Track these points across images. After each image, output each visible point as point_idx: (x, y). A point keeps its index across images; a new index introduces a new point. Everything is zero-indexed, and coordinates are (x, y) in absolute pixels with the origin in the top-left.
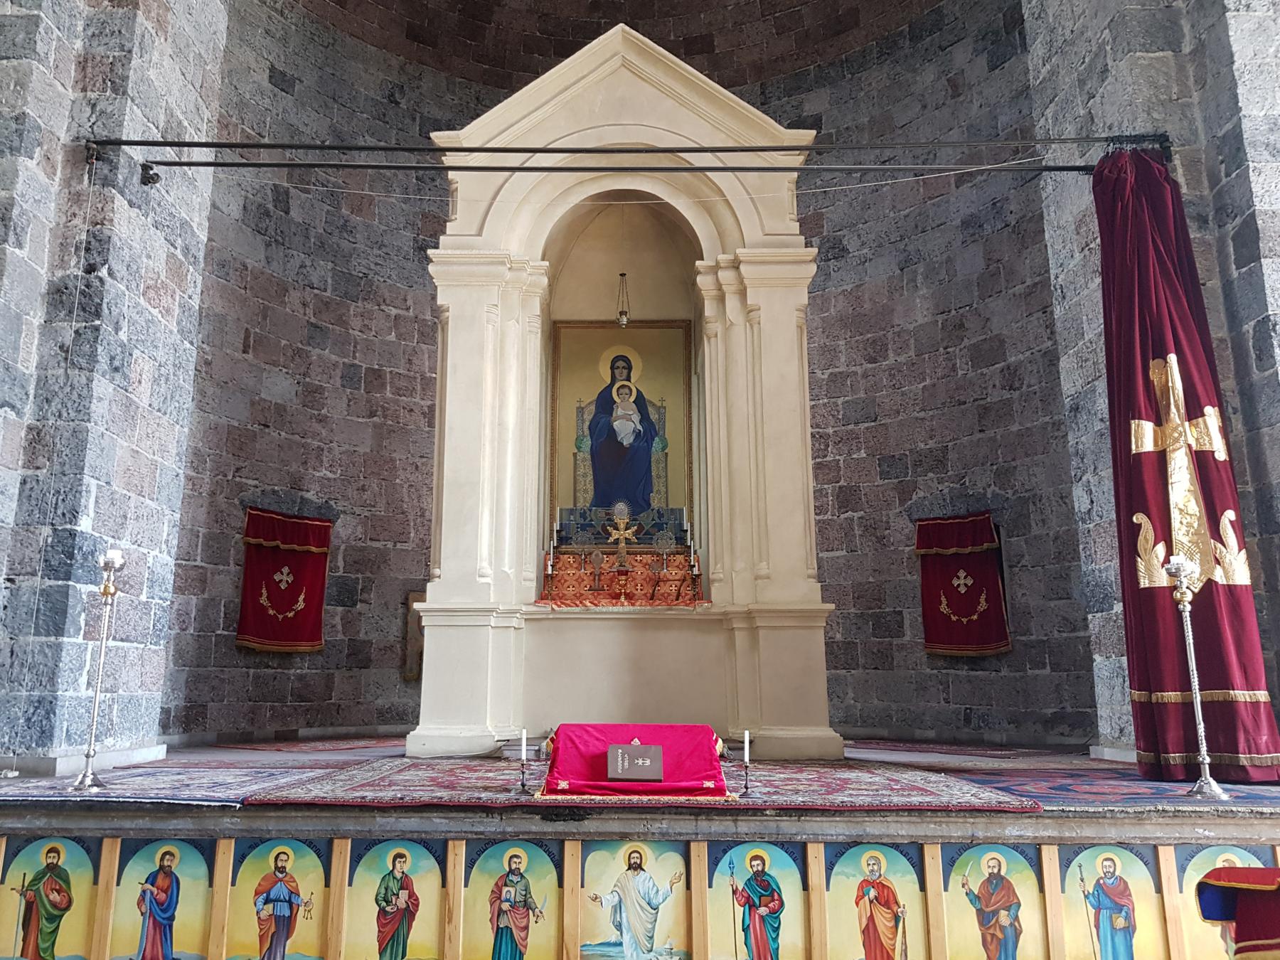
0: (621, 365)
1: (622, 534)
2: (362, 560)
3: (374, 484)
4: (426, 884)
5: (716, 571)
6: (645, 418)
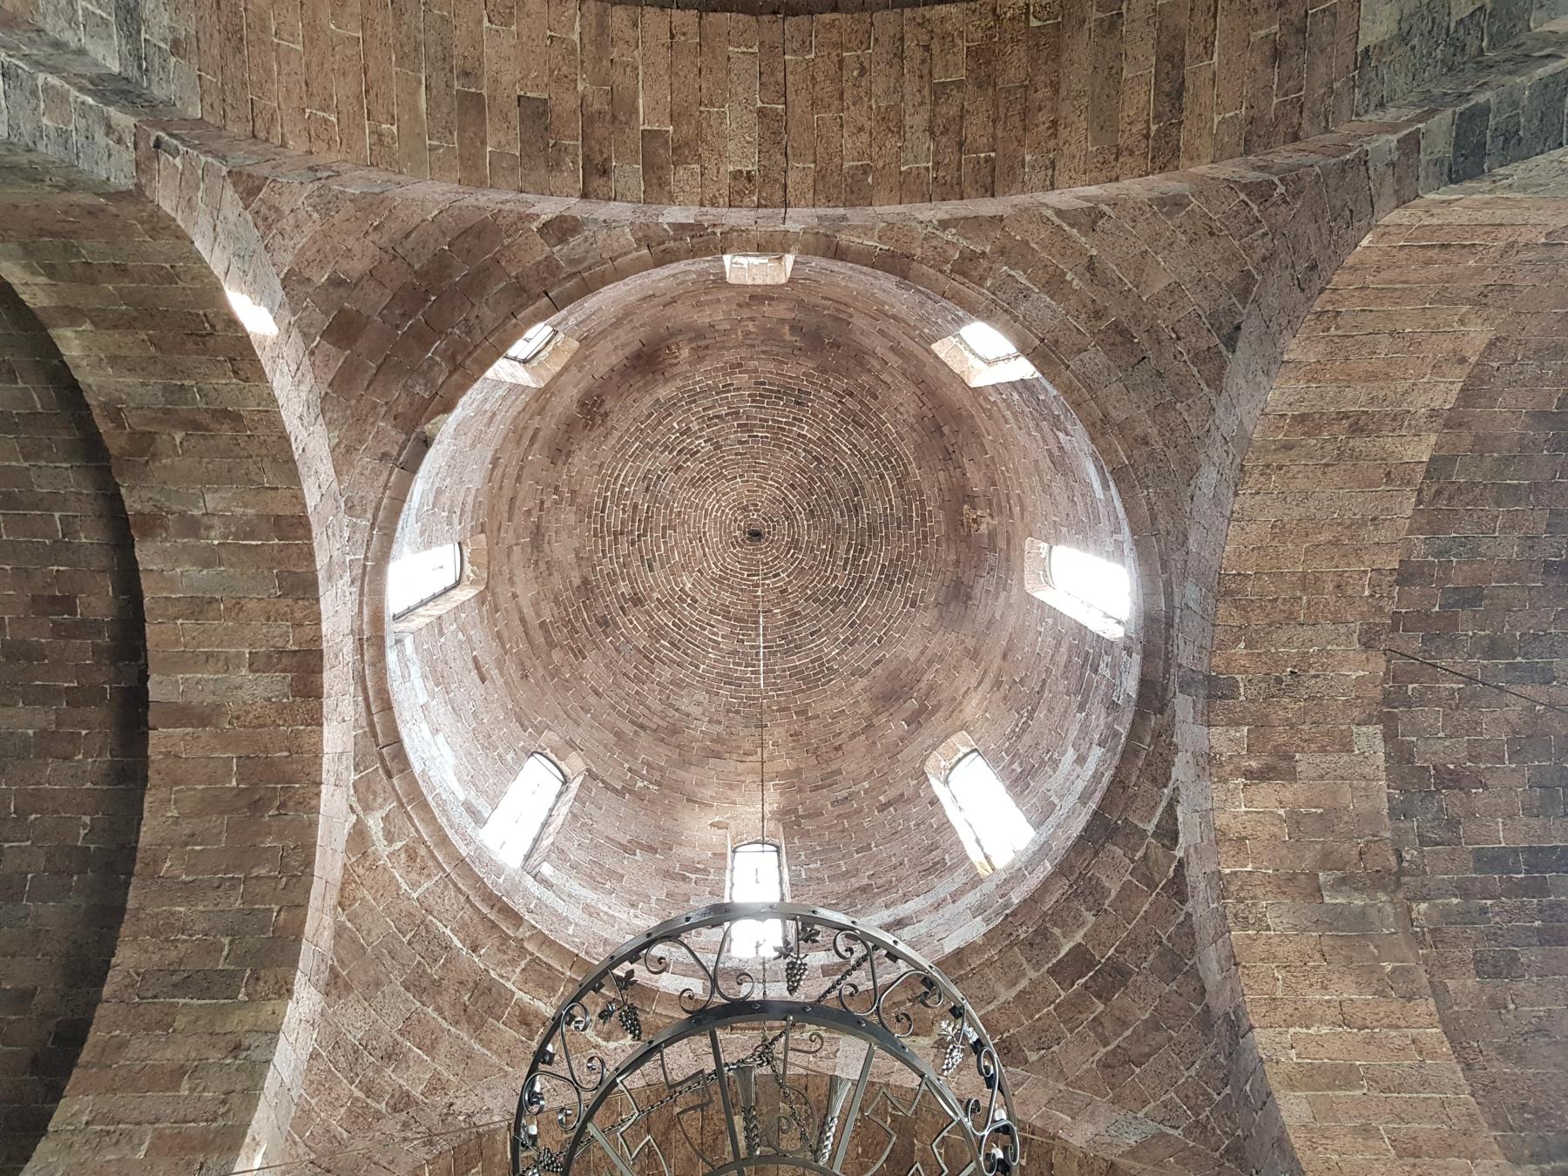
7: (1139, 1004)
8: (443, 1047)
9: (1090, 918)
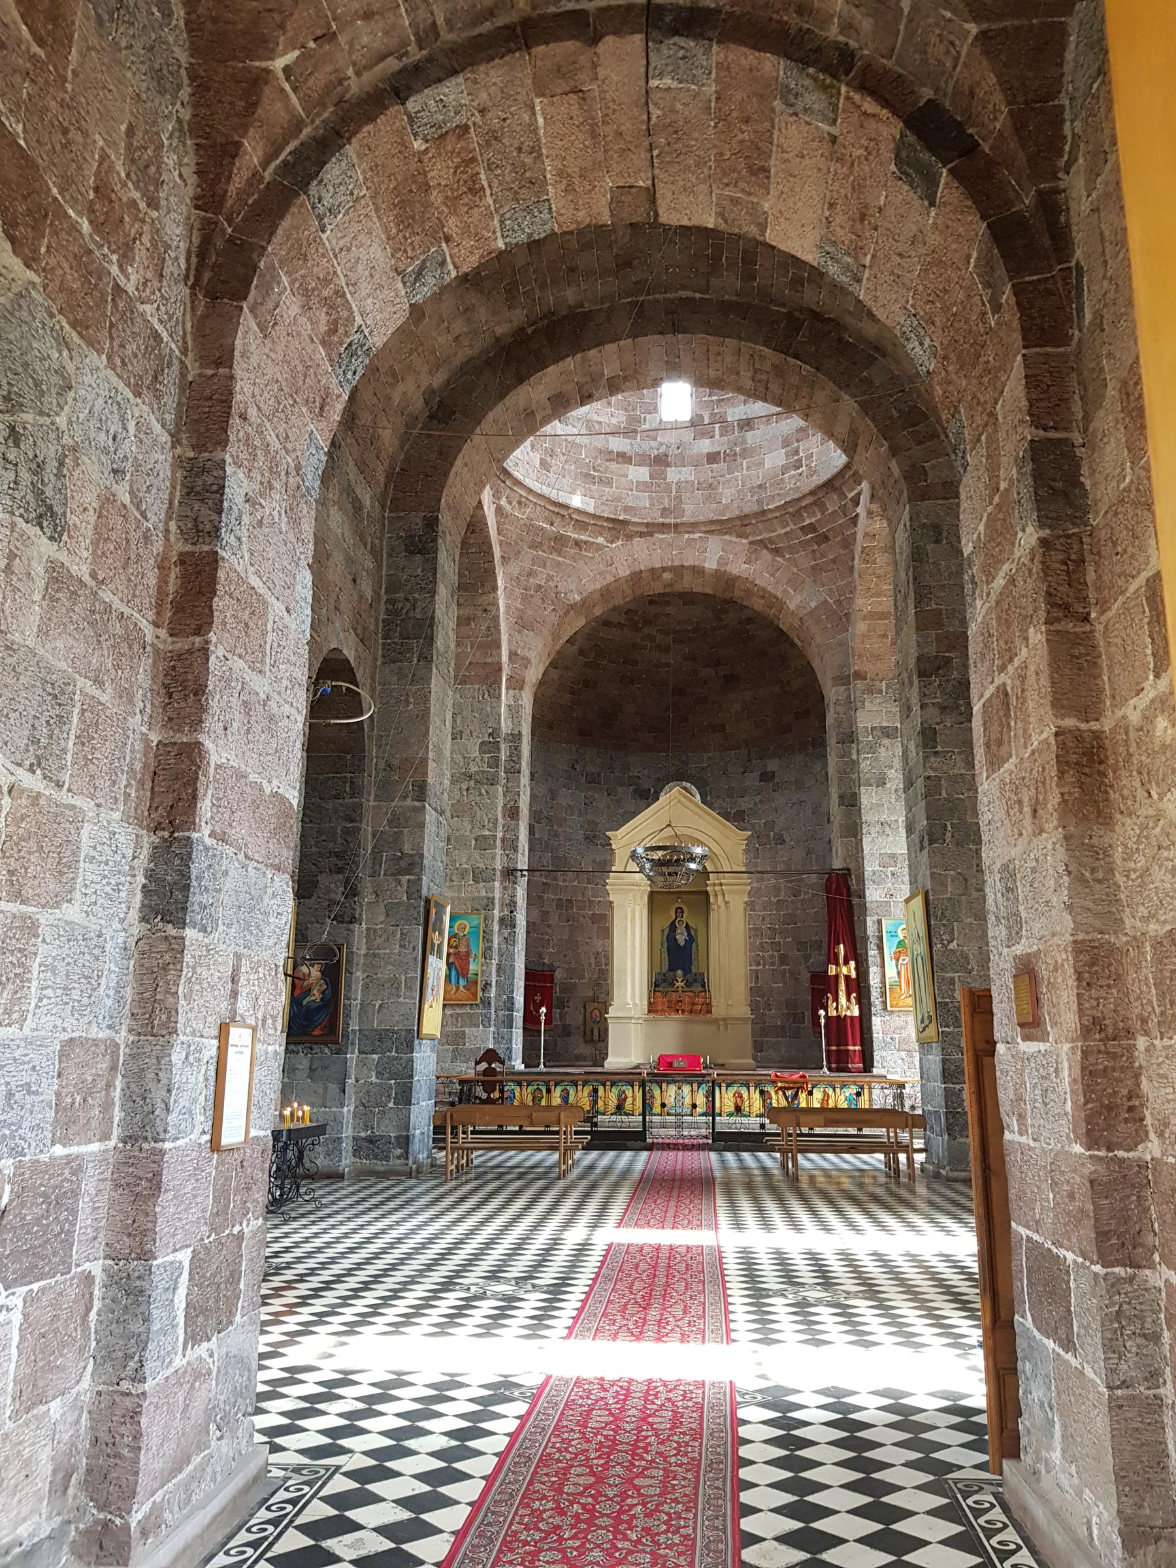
0: (679, 911)
1: (680, 984)
2: (567, 988)
3: (570, 953)
4: (629, 1093)
6: (689, 934)
7: (832, 551)
9: (819, 516)
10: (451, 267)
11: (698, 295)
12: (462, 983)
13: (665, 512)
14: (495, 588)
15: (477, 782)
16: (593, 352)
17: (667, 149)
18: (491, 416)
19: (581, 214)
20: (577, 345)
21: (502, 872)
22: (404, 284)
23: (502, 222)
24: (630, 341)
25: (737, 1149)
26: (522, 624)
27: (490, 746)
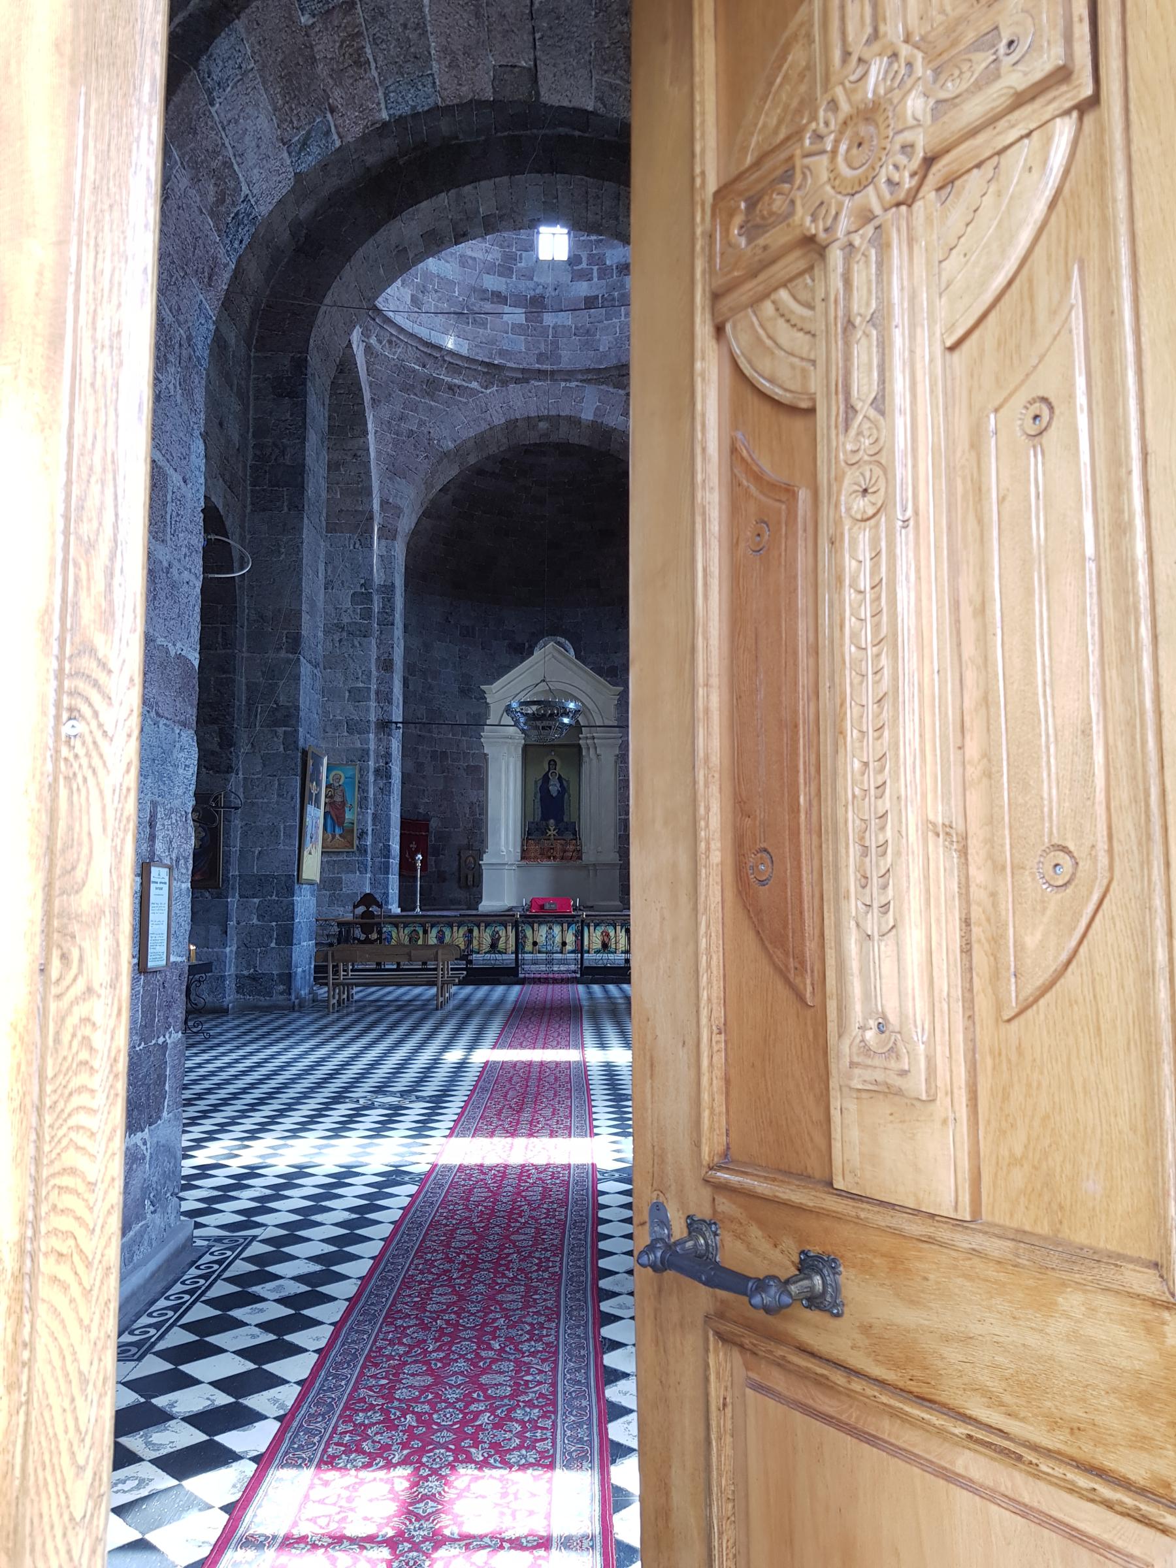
0: (552, 763)
4: (502, 933)
5: (584, 849)
6: (562, 785)
8: (420, 409)
10: (335, 137)
11: (577, 133)
12: (338, 831)
13: (540, 357)
14: (365, 433)
15: (349, 633)
16: (468, 189)
17: (549, 33)
18: (360, 253)
19: (464, 89)
20: (451, 183)
21: (377, 724)
22: (290, 153)
23: (386, 95)
24: (505, 179)
25: (603, 982)
26: (394, 471)
27: (363, 597)
